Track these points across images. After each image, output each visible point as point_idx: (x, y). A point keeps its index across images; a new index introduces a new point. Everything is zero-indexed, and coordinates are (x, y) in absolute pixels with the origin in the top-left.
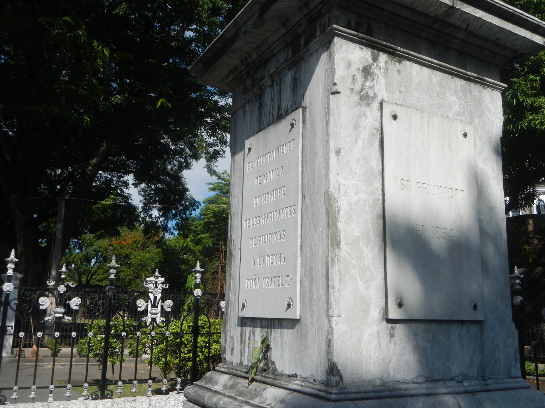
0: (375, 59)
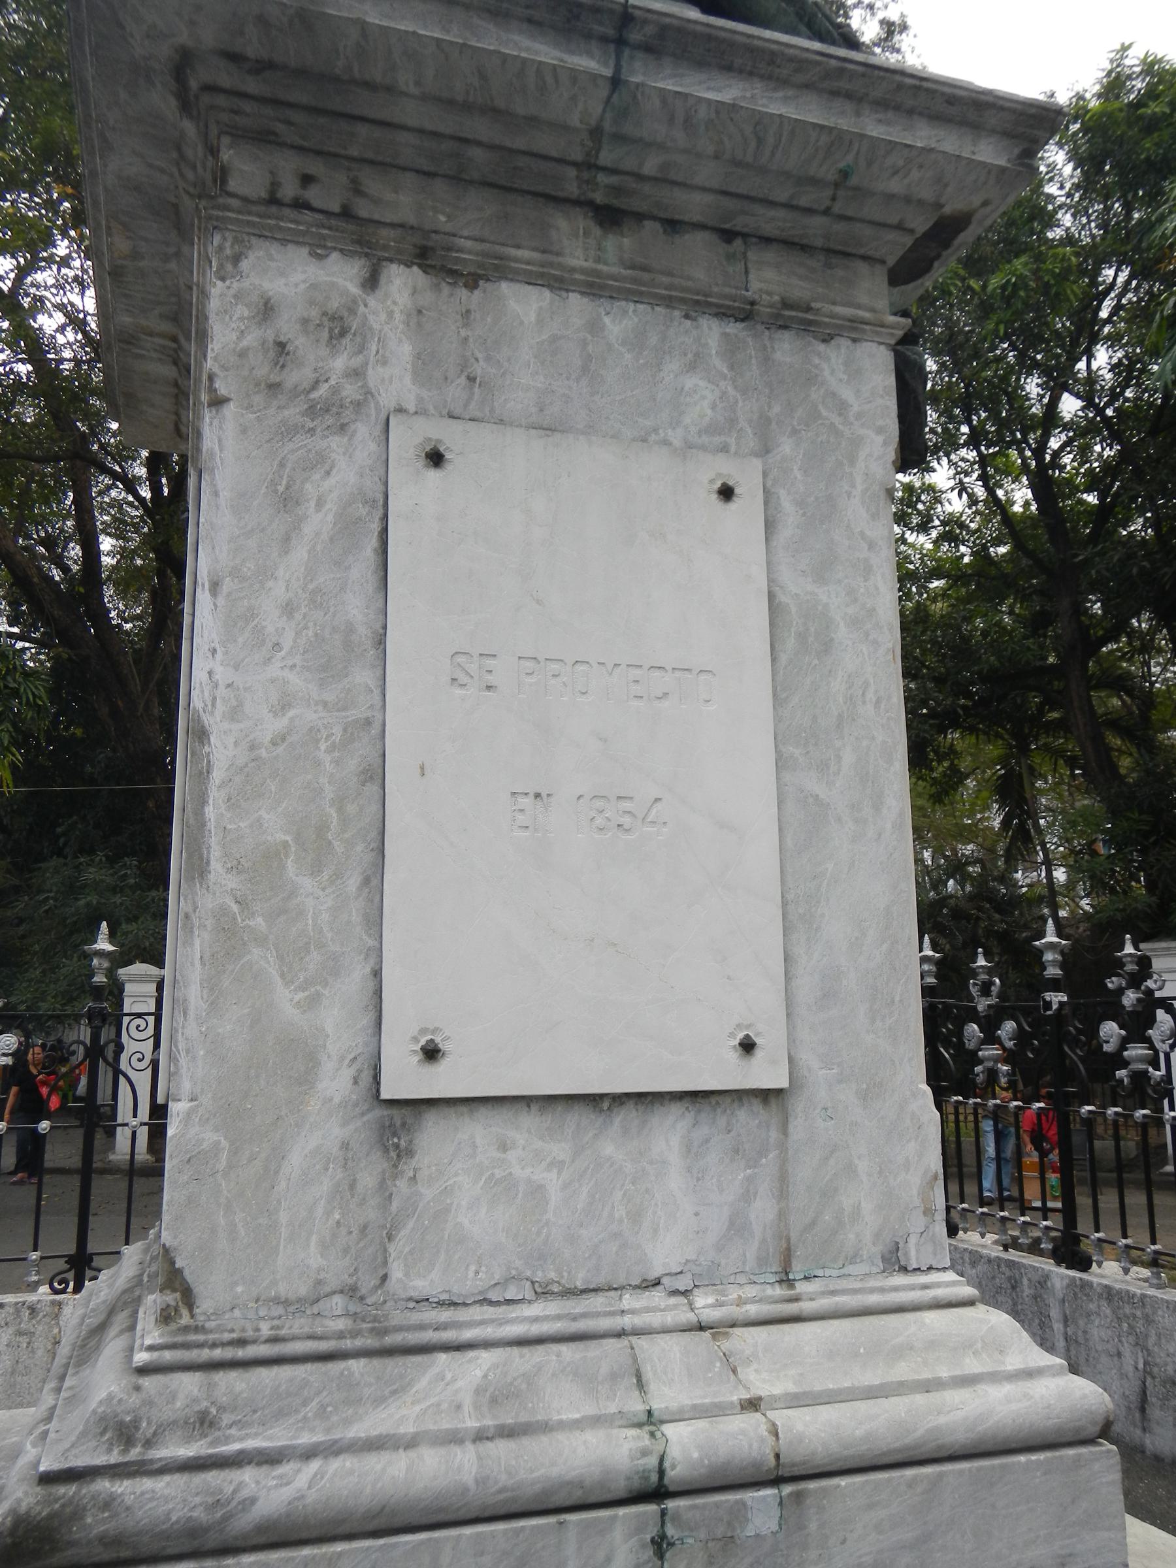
0: (372, 282)
